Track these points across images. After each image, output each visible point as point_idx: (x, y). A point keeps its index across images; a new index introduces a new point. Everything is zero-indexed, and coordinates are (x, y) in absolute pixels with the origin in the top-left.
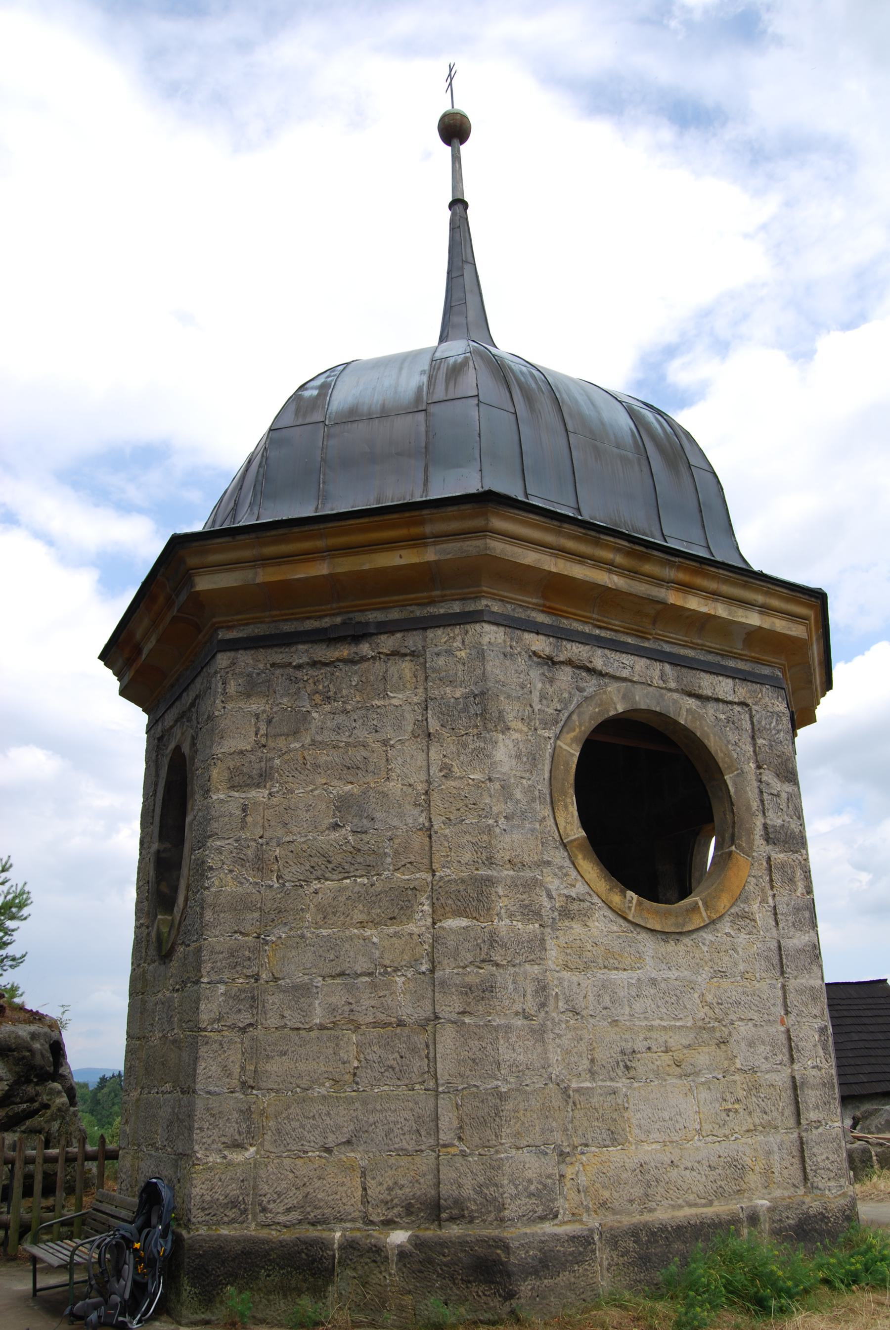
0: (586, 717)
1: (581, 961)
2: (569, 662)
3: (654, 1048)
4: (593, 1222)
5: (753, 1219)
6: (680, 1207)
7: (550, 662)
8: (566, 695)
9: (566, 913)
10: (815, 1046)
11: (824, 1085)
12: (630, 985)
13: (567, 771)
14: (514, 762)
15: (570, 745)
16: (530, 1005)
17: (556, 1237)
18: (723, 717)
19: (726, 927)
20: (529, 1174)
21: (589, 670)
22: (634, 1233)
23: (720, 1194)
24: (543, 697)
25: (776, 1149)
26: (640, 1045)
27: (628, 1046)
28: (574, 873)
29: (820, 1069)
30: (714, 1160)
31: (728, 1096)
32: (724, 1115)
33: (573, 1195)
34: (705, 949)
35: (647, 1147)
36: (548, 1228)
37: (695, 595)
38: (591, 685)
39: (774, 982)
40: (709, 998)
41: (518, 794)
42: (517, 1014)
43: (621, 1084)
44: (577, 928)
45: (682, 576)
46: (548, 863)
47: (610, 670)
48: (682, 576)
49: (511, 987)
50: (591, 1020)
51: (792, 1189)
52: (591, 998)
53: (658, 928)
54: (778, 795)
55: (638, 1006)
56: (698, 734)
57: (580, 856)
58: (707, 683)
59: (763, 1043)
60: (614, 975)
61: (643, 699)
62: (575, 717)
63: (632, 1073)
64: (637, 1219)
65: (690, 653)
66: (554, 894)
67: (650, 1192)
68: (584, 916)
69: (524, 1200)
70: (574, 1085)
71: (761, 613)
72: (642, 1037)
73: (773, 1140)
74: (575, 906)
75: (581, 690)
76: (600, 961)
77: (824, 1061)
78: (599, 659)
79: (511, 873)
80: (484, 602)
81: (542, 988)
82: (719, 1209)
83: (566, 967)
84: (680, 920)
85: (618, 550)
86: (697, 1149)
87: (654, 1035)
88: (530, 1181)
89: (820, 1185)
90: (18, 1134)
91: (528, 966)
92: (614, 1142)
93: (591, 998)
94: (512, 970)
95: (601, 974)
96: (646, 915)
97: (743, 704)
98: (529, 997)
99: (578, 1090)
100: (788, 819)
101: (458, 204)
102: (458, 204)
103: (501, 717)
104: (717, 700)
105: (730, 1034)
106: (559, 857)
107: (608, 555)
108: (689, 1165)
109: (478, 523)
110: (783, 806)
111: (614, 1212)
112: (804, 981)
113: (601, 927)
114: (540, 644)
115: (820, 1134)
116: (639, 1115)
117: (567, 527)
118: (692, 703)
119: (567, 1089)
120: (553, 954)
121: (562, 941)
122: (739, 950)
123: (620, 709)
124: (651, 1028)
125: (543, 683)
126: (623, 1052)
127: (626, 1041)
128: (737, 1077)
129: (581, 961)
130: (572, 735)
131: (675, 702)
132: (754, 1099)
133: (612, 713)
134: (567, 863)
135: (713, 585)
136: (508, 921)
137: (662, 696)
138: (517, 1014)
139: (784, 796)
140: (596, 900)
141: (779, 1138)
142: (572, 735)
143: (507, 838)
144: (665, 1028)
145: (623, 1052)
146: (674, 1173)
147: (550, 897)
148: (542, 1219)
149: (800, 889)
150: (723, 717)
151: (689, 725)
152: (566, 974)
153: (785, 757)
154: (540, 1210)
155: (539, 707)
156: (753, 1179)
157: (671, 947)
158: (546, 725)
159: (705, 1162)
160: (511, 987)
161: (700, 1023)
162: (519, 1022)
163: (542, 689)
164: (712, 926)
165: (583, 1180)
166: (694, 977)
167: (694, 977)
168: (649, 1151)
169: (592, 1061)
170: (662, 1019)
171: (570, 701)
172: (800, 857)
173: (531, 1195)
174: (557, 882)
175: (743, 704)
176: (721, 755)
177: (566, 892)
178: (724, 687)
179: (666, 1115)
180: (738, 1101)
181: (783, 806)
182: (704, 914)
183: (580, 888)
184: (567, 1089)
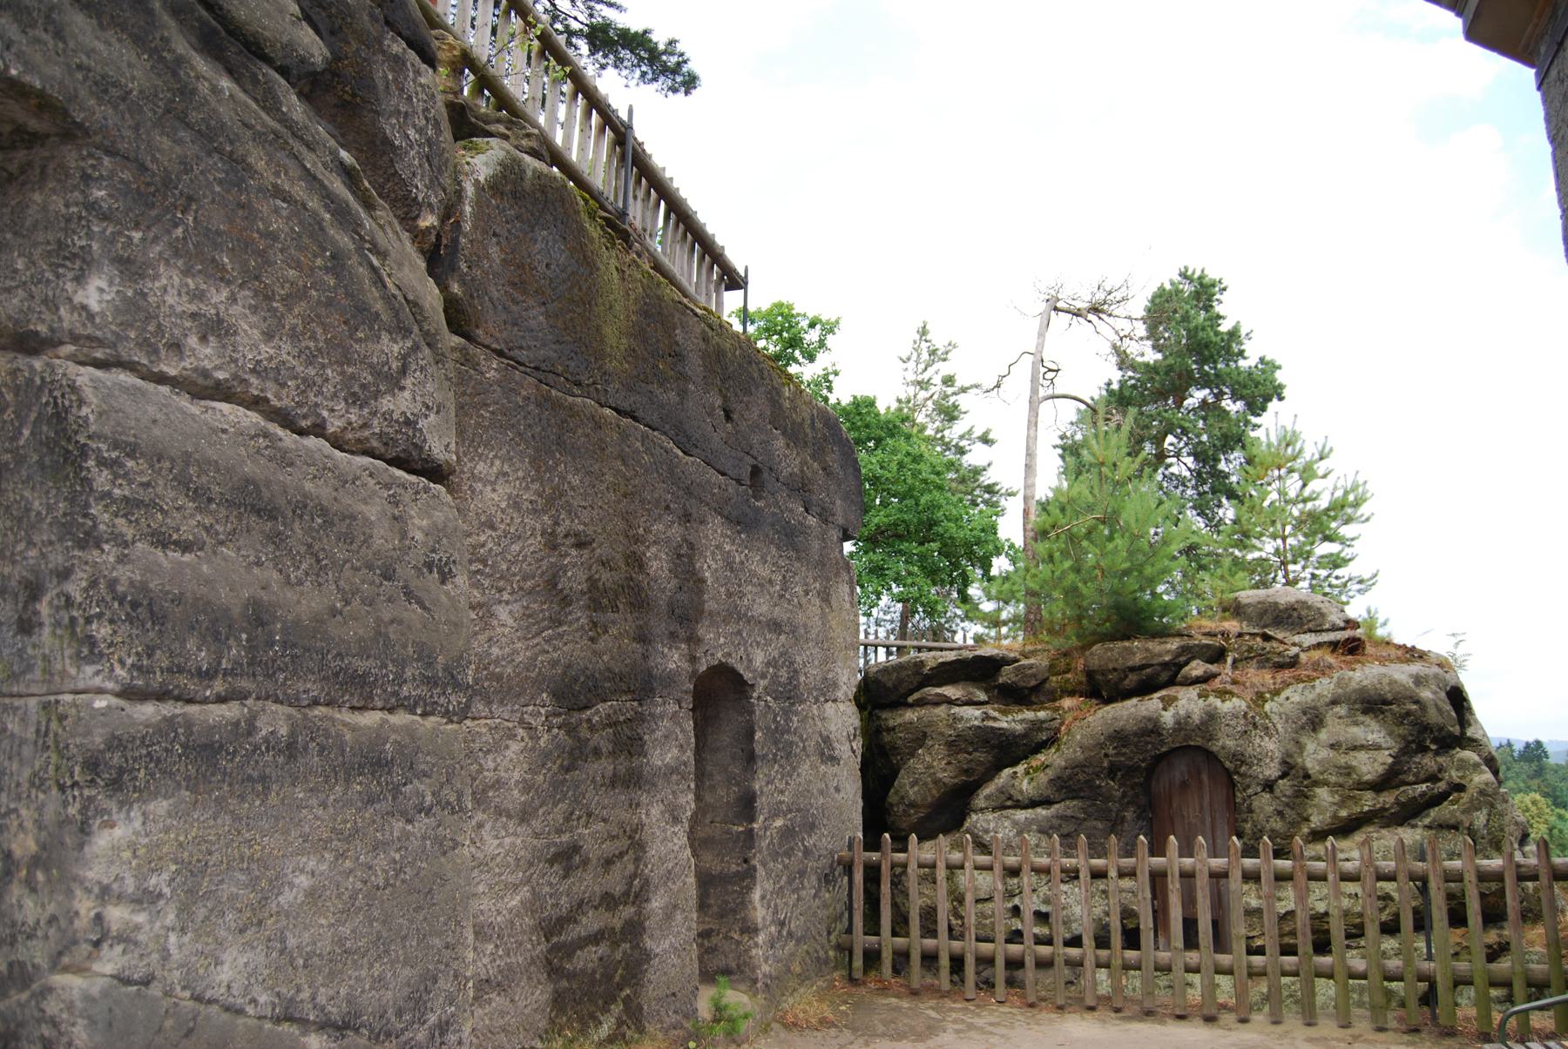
90: (1419, 831)
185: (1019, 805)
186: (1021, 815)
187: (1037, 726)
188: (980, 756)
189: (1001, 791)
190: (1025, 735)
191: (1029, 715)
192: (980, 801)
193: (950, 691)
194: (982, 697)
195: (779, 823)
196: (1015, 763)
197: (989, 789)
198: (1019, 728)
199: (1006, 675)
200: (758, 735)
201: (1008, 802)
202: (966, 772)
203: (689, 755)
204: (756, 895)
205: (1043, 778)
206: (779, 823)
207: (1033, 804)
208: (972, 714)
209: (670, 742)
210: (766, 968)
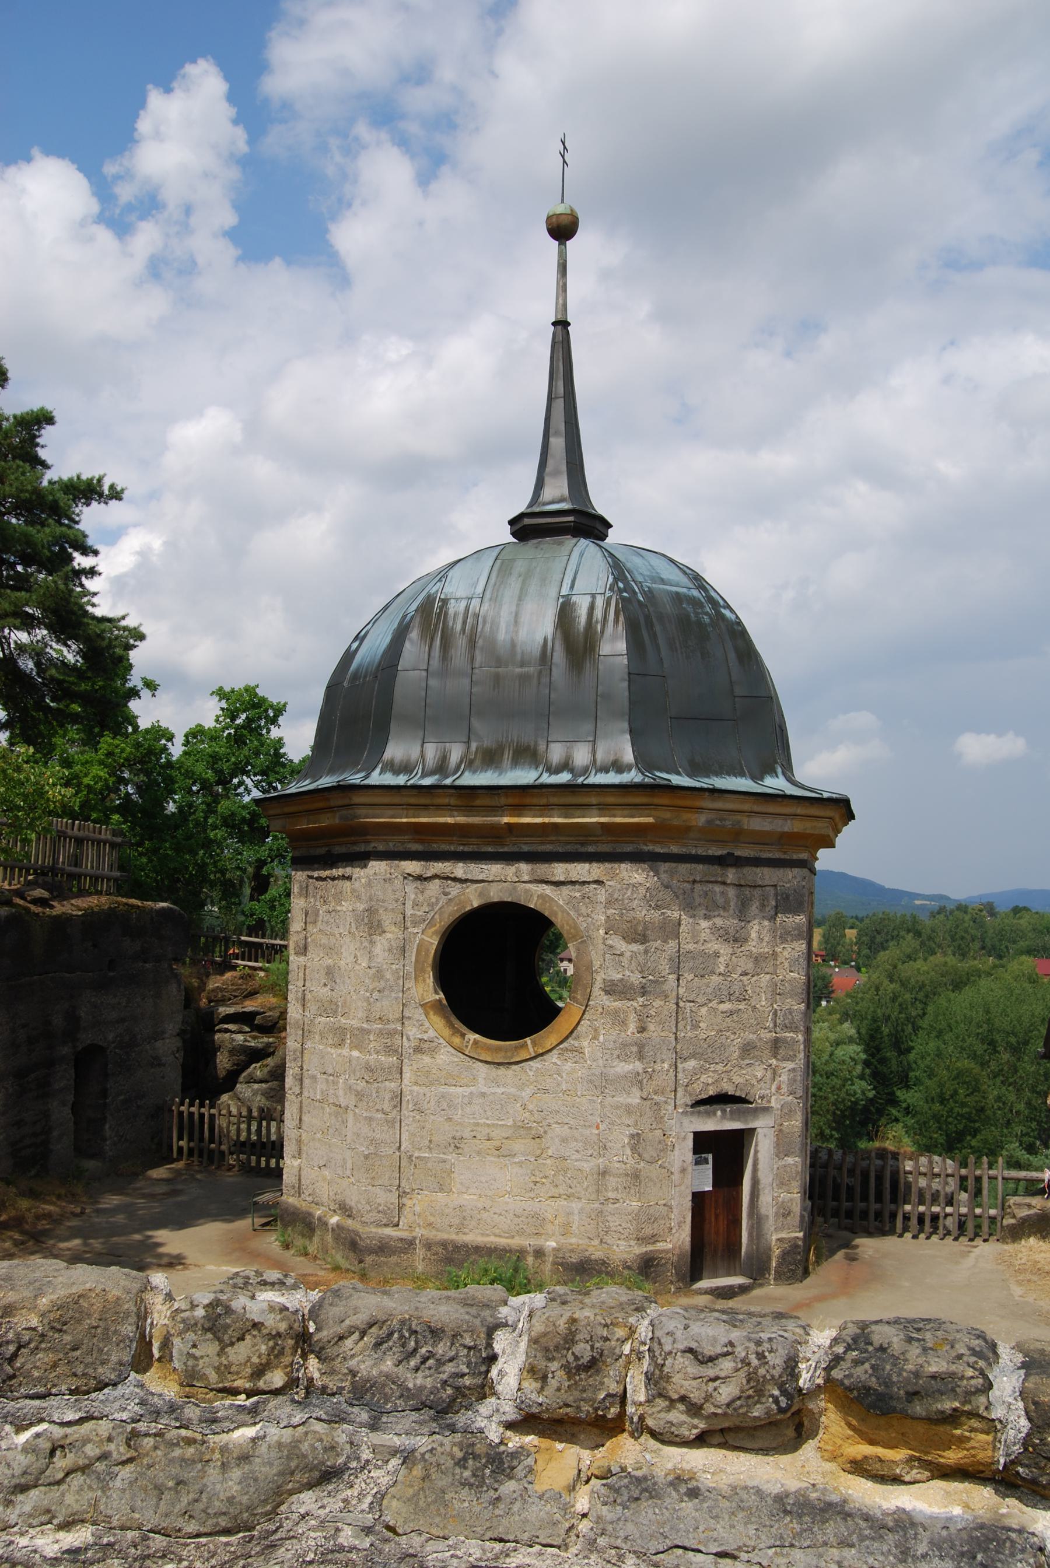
0: (446, 915)
1: (426, 1079)
2: (436, 876)
3: (479, 1137)
4: (418, 1232)
5: (539, 1253)
6: (488, 1235)
7: (420, 878)
8: (433, 900)
9: (418, 1050)
10: (623, 1147)
11: (627, 1175)
12: (464, 1096)
13: (427, 955)
14: (387, 954)
15: (431, 937)
16: (387, 1106)
17: (390, 1237)
18: (578, 895)
19: (554, 1057)
20: (378, 1201)
21: (455, 879)
22: (444, 1244)
23: (521, 1233)
24: (416, 904)
25: (576, 1212)
26: (467, 1134)
27: (458, 1135)
28: (427, 1024)
29: (626, 1164)
30: (519, 1212)
31: (537, 1173)
32: (532, 1185)
33: (410, 1216)
34: (531, 1073)
35: (466, 1196)
36: (388, 1231)
37: (530, 810)
38: (455, 889)
39: (595, 1098)
40: (530, 1107)
41: (388, 976)
42: (378, 1110)
43: (451, 1157)
44: (427, 1059)
45: (511, 801)
46: (409, 1018)
47: (469, 877)
48: (511, 801)
49: (374, 1095)
50: (432, 1117)
51: (587, 1240)
52: (432, 1103)
53: (489, 1059)
54: (622, 955)
55: (468, 1110)
56: (546, 914)
57: (431, 1013)
58: (560, 870)
59: (576, 1140)
60: (452, 1089)
61: (496, 894)
62: (437, 916)
63: (460, 1151)
64: (454, 1237)
65: (548, 848)
66: (411, 1038)
67: (465, 1223)
68: (433, 1051)
69: (375, 1214)
70: (416, 1154)
71: (599, 809)
72: (469, 1129)
73: (576, 1206)
74: (426, 1045)
75: (446, 894)
76: (442, 1081)
77: (630, 1158)
78: (460, 869)
79: (380, 1026)
80: (372, 845)
81: (398, 1098)
82: (516, 1242)
83: (416, 1083)
84: (509, 1054)
85: (451, 795)
86: (507, 1203)
87: (479, 1129)
88: (379, 1205)
89: (609, 1242)
91: (387, 1083)
92: (441, 1190)
93: (432, 1103)
94: (376, 1085)
95: (442, 1089)
96: (479, 1050)
97: (598, 882)
98: (386, 1101)
99: (417, 1158)
100: (627, 973)
101: (562, 324)
102: (562, 324)
103: (379, 924)
104: (573, 883)
105: (545, 1132)
106: (419, 1014)
107: (446, 801)
108: (498, 1212)
109: (346, 802)
110: (625, 963)
111: (438, 1230)
112: (621, 1099)
113: (446, 1057)
114: (412, 867)
115: (617, 1208)
116: (462, 1177)
117: (404, 792)
118: (548, 890)
119: (411, 1156)
120: (407, 1075)
121: (415, 1067)
122: (564, 1075)
123: (476, 905)
124: (477, 1124)
125: (416, 894)
126: (454, 1138)
127: (457, 1131)
128: (549, 1161)
129: (426, 1079)
130: (433, 929)
131: (527, 891)
132: (561, 1177)
133: (468, 908)
134: (423, 1017)
135: (544, 801)
136: (375, 1056)
137: (515, 888)
138: (378, 1110)
139: (628, 954)
140: (441, 1041)
141: (580, 1205)
142: (433, 929)
143: (378, 1004)
144: (488, 1125)
145: (454, 1138)
146: (485, 1215)
147: (409, 1039)
148: (386, 1225)
149: (632, 1027)
150: (578, 895)
151: (538, 908)
152: (416, 1088)
153: (635, 922)
154: (385, 1221)
155: (412, 912)
156: (549, 1227)
157: (502, 1071)
158: (415, 924)
159: (512, 1212)
160: (374, 1095)
161: (520, 1124)
162: (379, 1115)
163: (414, 899)
164: (539, 1059)
165: (417, 1209)
166: (518, 1093)
167: (518, 1093)
168: (468, 1199)
169: (430, 1141)
170: (487, 1119)
171: (437, 904)
172: (635, 1004)
173: (379, 1212)
174: (414, 1030)
175: (598, 882)
176: (566, 927)
177: (420, 1036)
178: (580, 870)
179: (483, 1179)
180: (546, 1177)
181: (625, 963)
182: (531, 1050)
183: (431, 1033)
184: (411, 1156)
185: (255, 1082)
186: (256, 1086)
187: (269, 1045)
188: (242, 1058)
189: (249, 1075)
190: (263, 1049)
191: (266, 1040)
192: (241, 1079)
193: (231, 1027)
194: (248, 1029)
195: (122, 1098)
196: (257, 1062)
197: (244, 1074)
198: (260, 1045)
199: (258, 1020)
200: (110, 1066)
201: (251, 1080)
202: (237, 1065)
203: (72, 1082)
204: (107, 1126)
205: (266, 1070)
206: (122, 1098)
207: (261, 1082)
208: (240, 1037)
209: (64, 1078)
210: (111, 1154)
